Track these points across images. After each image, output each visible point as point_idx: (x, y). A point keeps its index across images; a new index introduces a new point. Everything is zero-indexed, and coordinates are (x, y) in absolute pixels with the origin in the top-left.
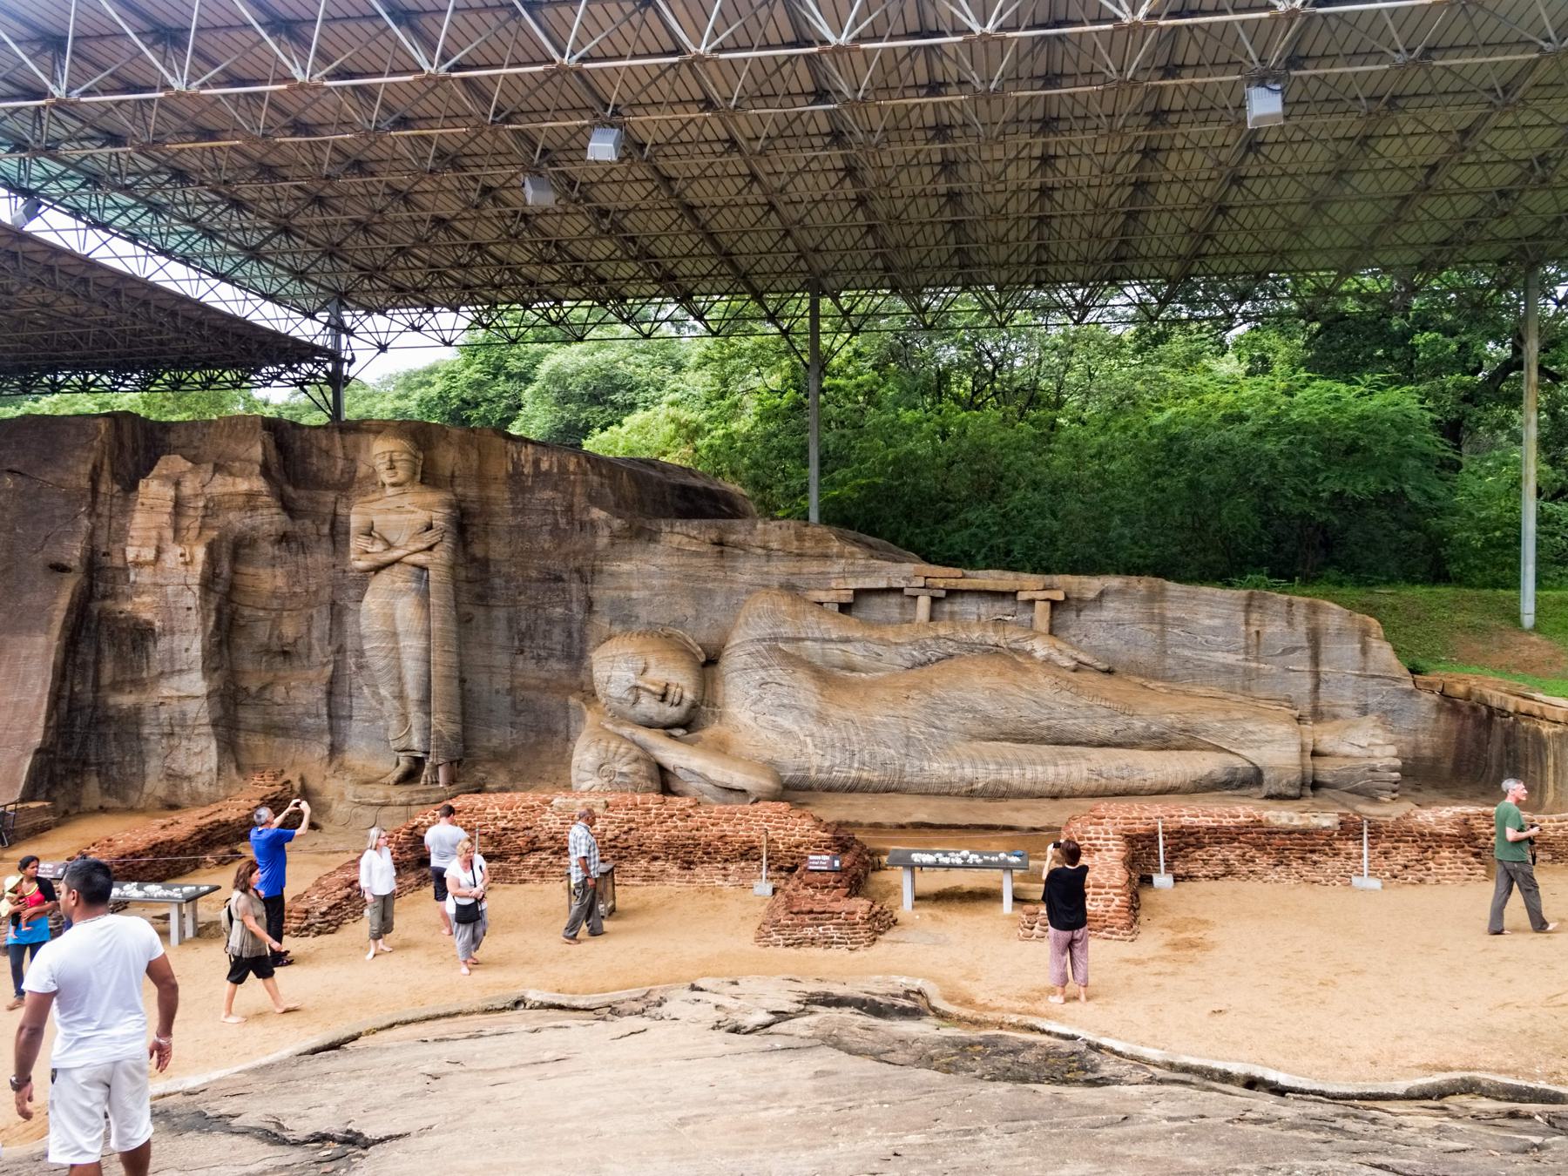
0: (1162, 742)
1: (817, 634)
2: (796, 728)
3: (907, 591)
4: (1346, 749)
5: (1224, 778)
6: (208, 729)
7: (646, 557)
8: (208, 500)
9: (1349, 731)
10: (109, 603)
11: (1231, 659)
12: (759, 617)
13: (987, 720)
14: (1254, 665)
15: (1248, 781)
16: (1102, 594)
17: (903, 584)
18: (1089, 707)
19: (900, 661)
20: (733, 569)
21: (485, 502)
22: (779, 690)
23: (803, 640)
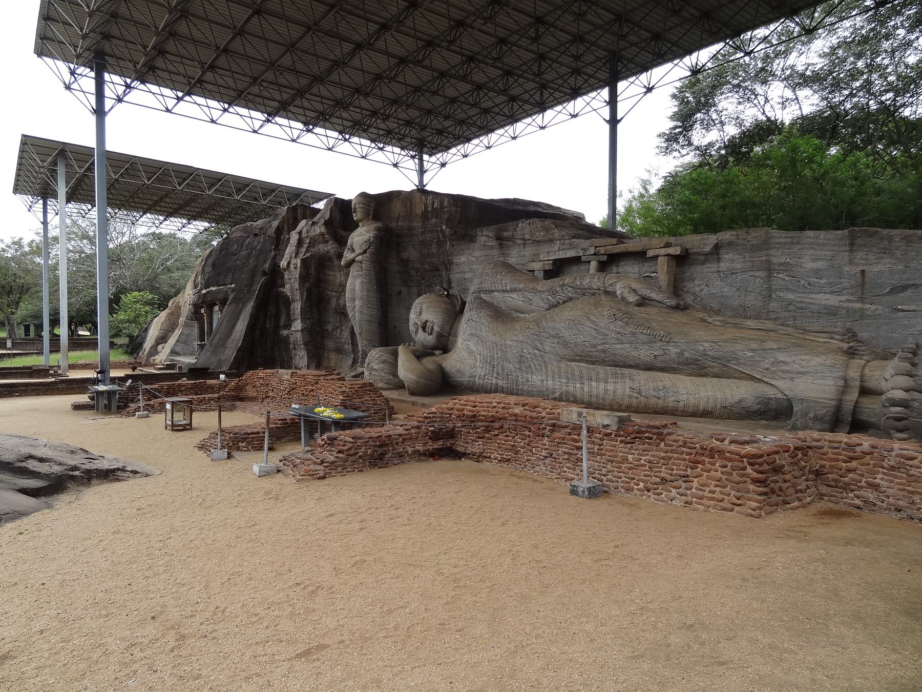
0: (697, 368)
1: (500, 288)
3: (583, 259)
5: (757, 407)
6: (303, 346)
7: (470, 252)
8: (311, 239)
10: (281, 289)
11: (834, 300)
13: (565, 344)
14: (858, 305)
15: (777, 413)
16: (717, 248)
18: (633, 334)
21: (410, 229)
23: (493, 291)
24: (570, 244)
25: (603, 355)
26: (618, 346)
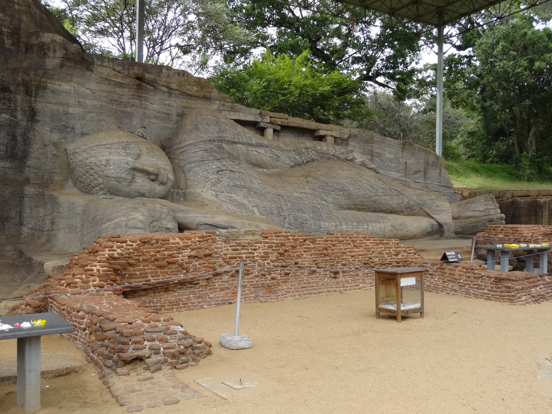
0: (410, 211)
1: (244, 140)
2: (245, 202)
4: (470, 214)
9: (469, 205)
11: (396, 175)
12: (207, 124)
13: (349, 196)
14: (404, 179)
17: (259, 120)
18: (390, 189)
19: (288, 161)
20: (146, 99)
22: (232, 175)
23: (236, 143)
24: (232, 108)
25: (373, 204)
26: (384, 197)
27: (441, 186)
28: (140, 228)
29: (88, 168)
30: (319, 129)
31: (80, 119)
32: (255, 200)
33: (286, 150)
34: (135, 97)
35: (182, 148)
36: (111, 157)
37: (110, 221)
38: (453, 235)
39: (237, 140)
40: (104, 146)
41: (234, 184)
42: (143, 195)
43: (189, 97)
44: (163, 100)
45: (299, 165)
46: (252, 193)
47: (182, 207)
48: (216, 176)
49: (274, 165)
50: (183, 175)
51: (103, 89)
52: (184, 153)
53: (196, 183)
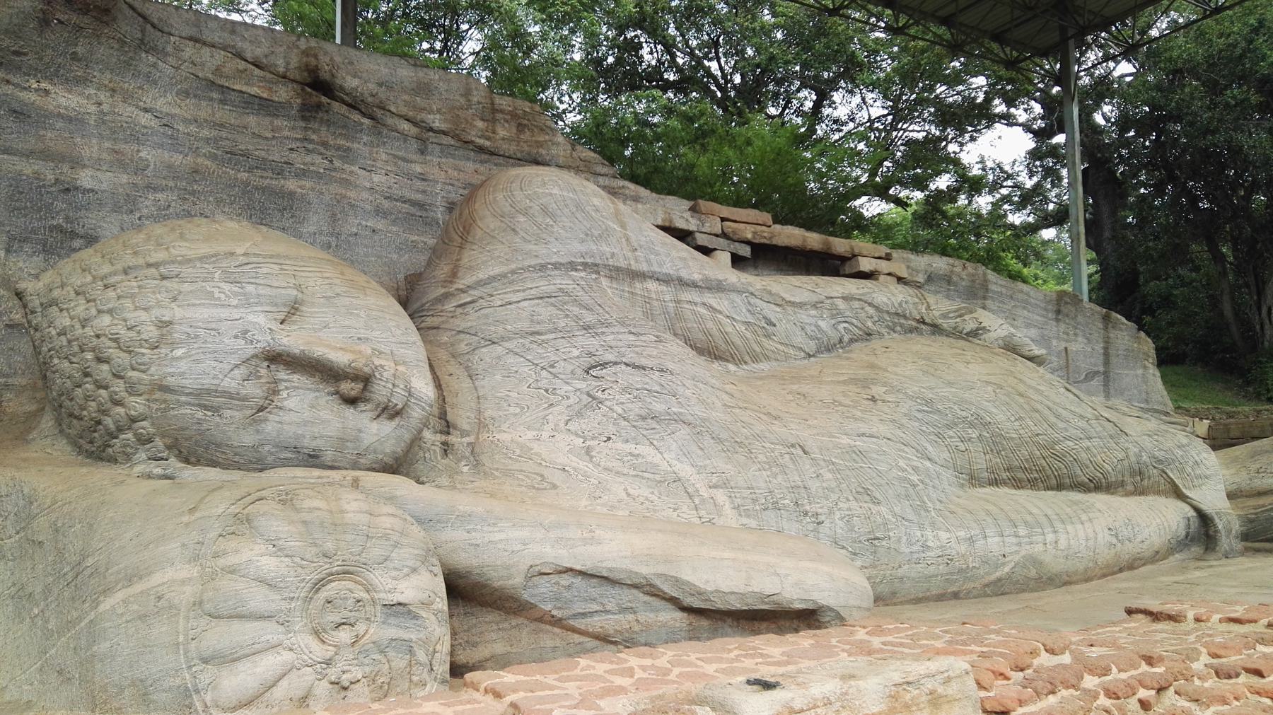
1: (668, 269)
2: (685, 470)
7: (130, 84)
13: (995, 443)
17: (692, 228)
19: (799, 339)
20: (347, 155)
22: (636, 378)
23: (642, 276)
26: (1086, 443)
27: (1149, 410)
28: (262, 617)
29: (89, 356)
30: (854, 256)
31: (116, 209)
32: (721, 464)
33: (792, 304)
34: (310, 146)
35: (463, 291)
36: (178, 313)
37: (130, 580)
38: (1239, 545)
39: (644, 267)
40: (153, 271)
41: (643, 413)
42: (312, 459)
43: (484, 157)
44: (404, 160)
45: (829, 349)
46: (707, 441)
47: (464, 502)
48: (582, 385)
49: (758, 349)
50: (466, 383)
51: (202, 115)
52: (468, 309)
53: (512, 410)
